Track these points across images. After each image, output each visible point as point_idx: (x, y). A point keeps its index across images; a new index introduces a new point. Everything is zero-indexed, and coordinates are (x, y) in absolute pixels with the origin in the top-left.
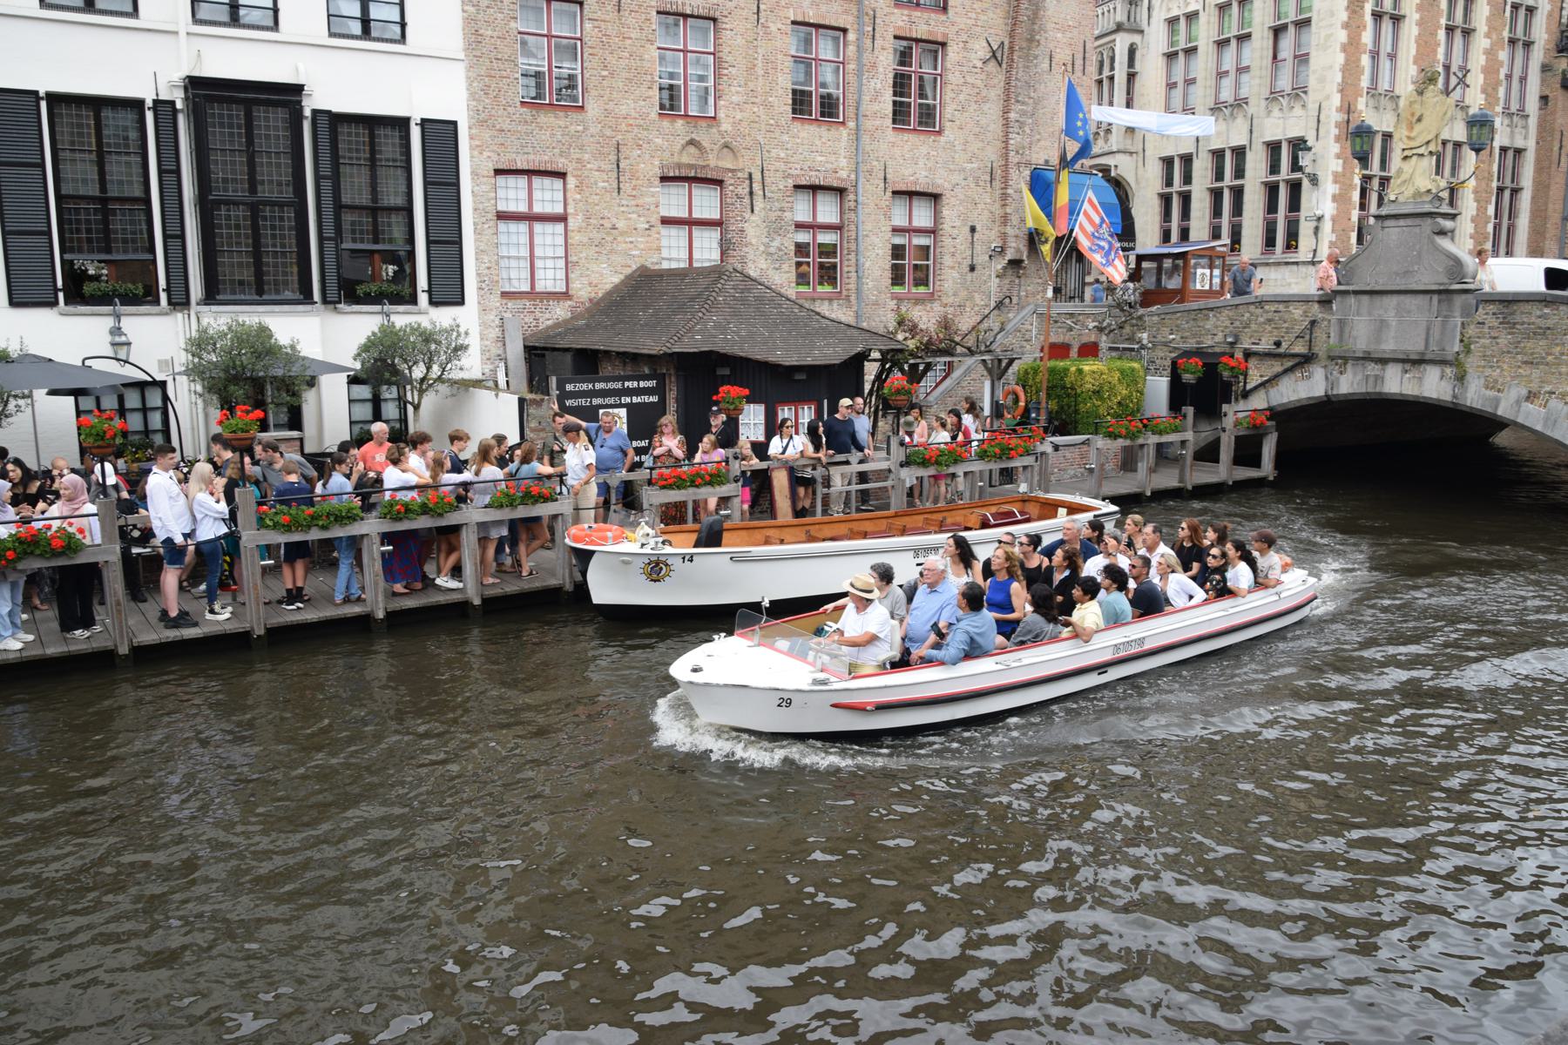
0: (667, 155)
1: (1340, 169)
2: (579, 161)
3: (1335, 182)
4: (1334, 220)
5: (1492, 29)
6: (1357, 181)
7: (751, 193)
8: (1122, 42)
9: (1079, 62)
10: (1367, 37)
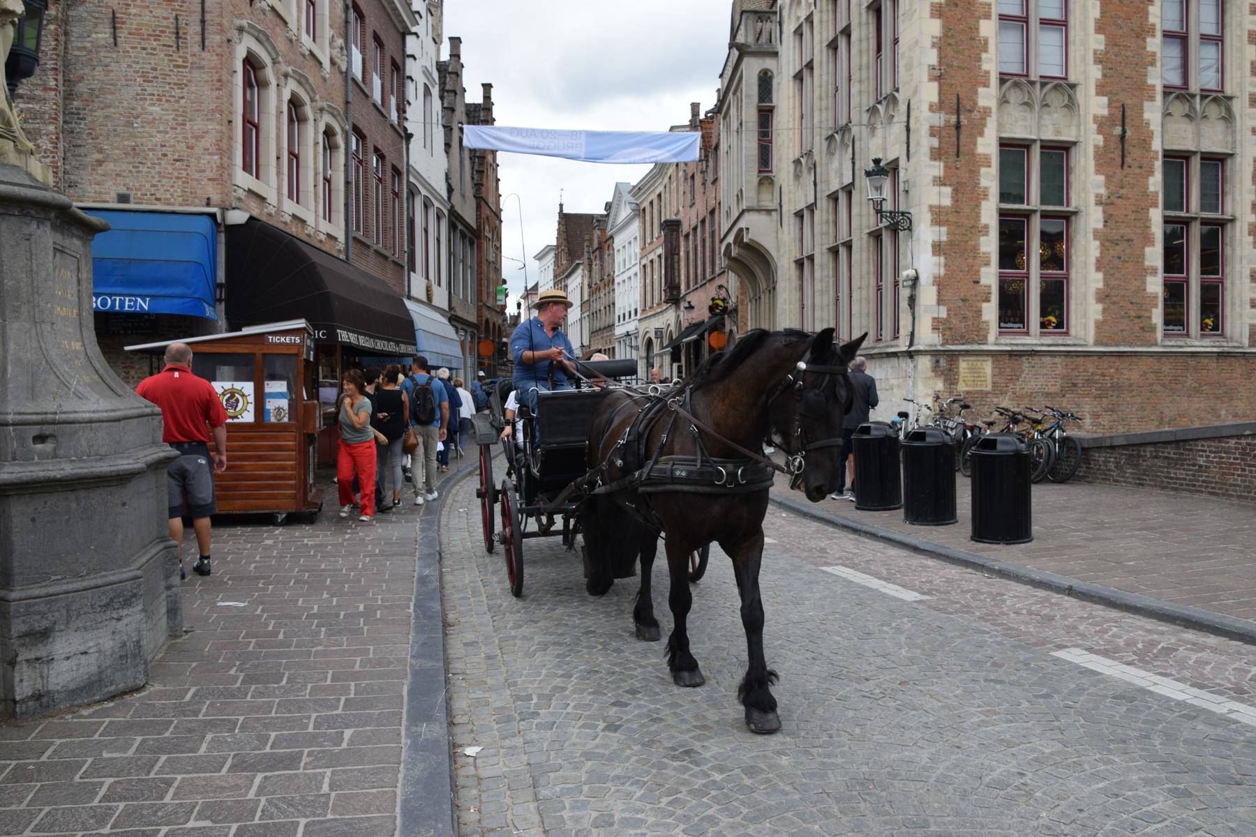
1: (947, 202)
4: (939, 283)
8: (752, 68)
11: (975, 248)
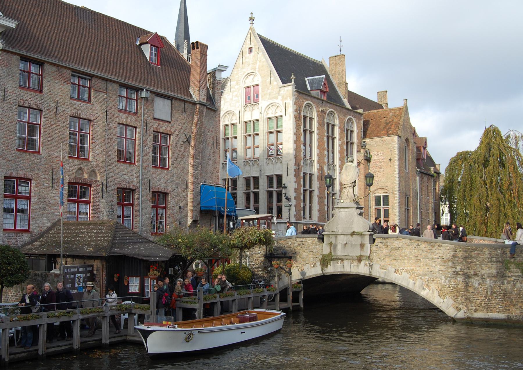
0: (71, 173)
2: (38, 174)
3: (295, 192)
4: (295, 206)
6: (302, 191)
7: (102, 190)
9: (215, 144)
10: (302, 138)
11: (300, 198)
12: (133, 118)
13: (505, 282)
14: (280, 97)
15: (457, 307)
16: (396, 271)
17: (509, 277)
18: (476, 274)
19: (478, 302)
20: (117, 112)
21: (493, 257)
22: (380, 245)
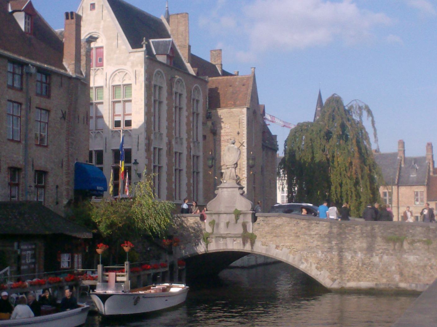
5: (188, 108)
6: (152, 168)
9: (85, 120)
10: (152, 110)
12: (20, 94)
13: (374, 254)
14: (129, 64)
15: (333, 278)
16: (277, 247)
17: (377, 250)
18: (349, 249)
19: (351, 273)
20: (6, 89)
21: (364, 233)
22: (262, 223)
